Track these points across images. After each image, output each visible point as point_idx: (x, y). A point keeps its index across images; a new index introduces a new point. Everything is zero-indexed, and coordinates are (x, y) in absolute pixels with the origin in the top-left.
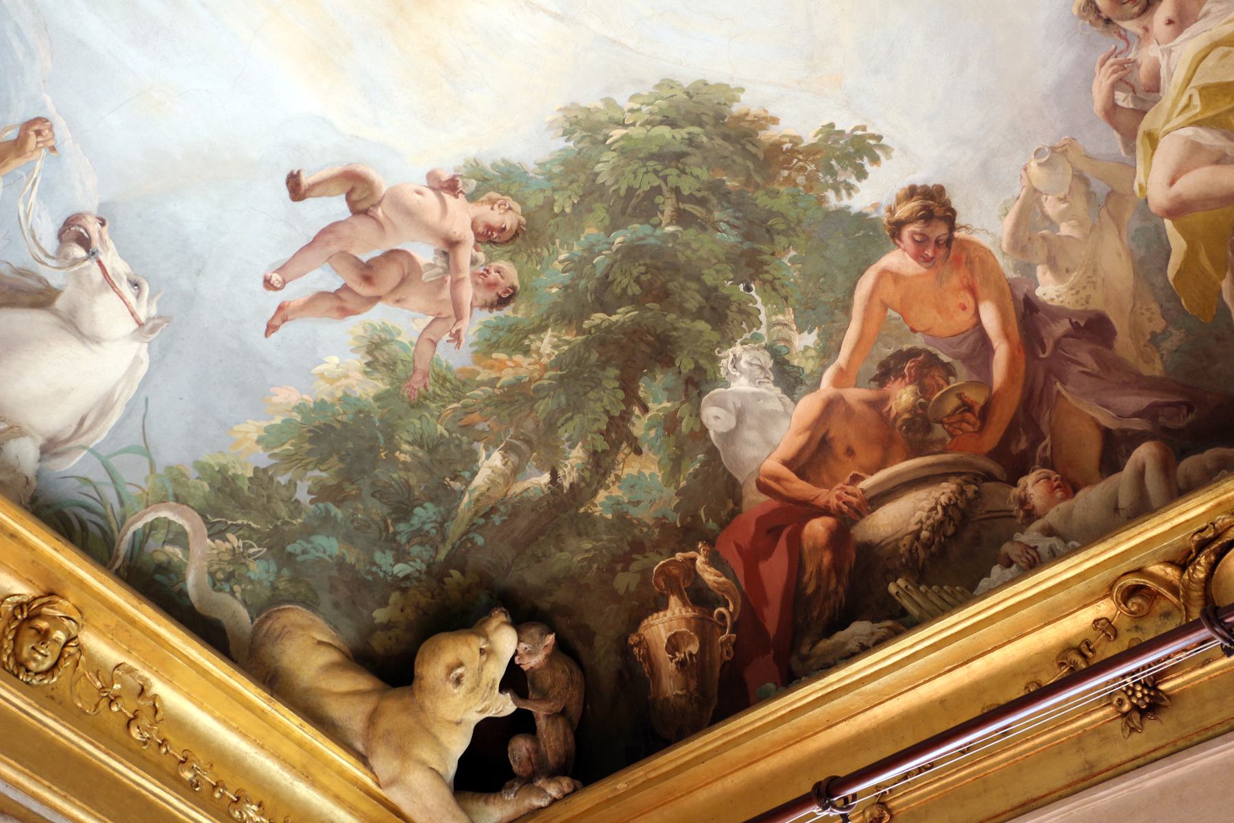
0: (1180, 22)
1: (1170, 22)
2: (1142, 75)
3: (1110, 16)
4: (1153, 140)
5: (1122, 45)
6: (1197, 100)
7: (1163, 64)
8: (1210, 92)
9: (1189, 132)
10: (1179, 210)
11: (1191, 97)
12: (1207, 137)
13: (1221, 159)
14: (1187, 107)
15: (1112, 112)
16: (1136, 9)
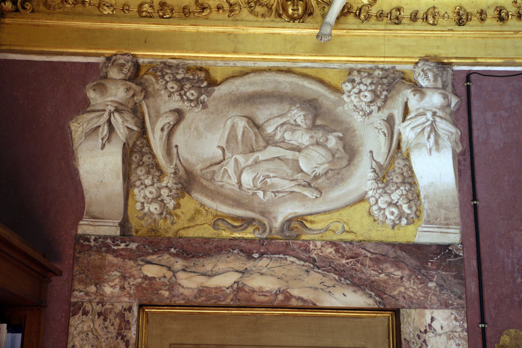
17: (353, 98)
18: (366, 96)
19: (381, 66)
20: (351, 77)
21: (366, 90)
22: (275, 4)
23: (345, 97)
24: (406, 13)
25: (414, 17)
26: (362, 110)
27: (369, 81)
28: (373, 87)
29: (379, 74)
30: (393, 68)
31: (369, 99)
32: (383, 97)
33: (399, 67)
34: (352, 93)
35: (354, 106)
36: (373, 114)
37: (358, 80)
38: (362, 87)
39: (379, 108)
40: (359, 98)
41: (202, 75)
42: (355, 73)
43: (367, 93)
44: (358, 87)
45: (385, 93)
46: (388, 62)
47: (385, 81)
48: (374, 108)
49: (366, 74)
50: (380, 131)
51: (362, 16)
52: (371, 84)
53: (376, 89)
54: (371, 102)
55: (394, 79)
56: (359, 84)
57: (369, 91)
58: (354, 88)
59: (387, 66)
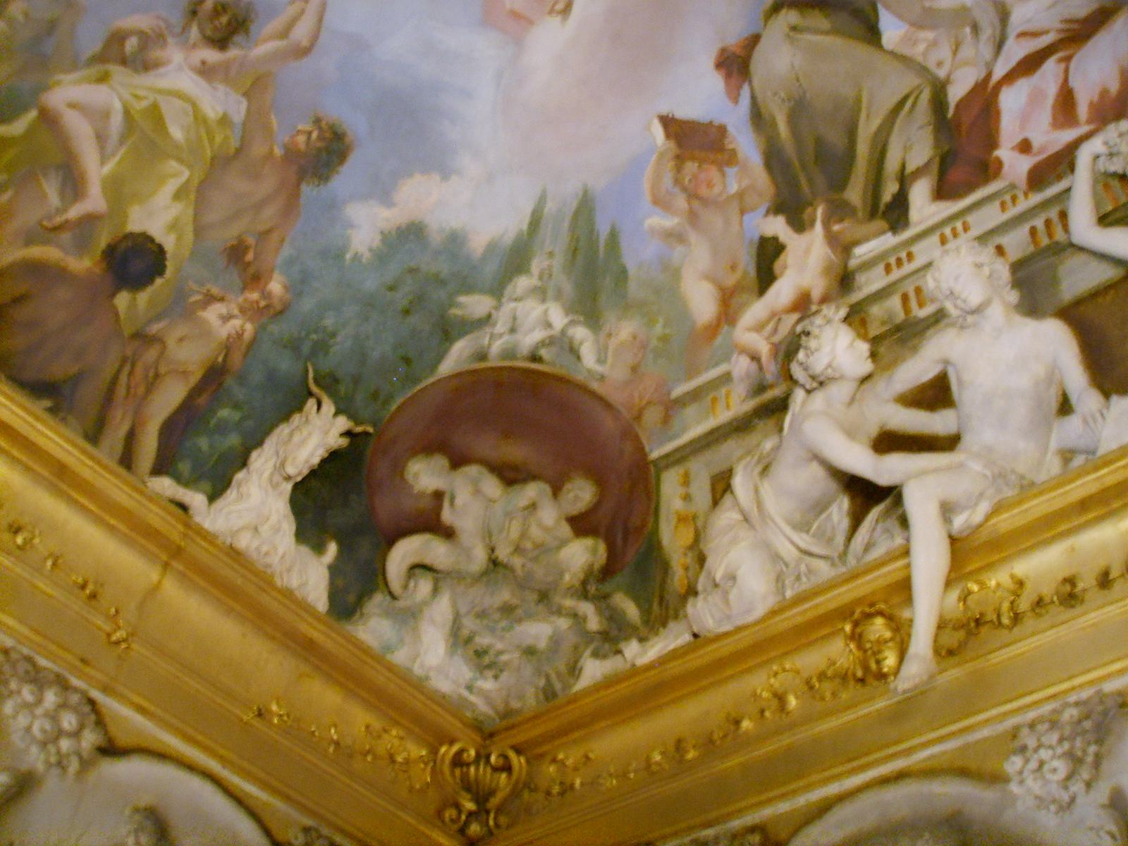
0: (205, 71)
1: (203, 63)
2: (156, 54)
3: (200, 14)
4: (103, 79)
5: (178, 30)
6: (144, 104)
7: (171, 67)
8: (155, 114)
9: (118, 105)
10: (48, 119)
11: (145, 98)
12: (117, 120)
13: (101, 138)
14: (136, 96)
15: (118, 38)
16: (209, 33)
17: (1030, 782)
18: (1055, 770)
19: (1073, 698)
20: (1017, 743)
21: (1053, 757)
22: (852, 667)
23: (1014, 788)
24: (1087, 582)
25: (1105, 581)
26: (1054, 801)
27: (1053, 738)
28: (1066, 746)
29: (1072, 716)
30: (1099, 692)
31: (1062, 772)
32: (1090, 759)
33: (1109, 687)
34: (1026, 774)
35: (1037, 797)
36: (1079, 800)
37: (1031, 743)
38: (1044, 754)
39: (1088, 785)
40: (1043, 778)
41: (756, 839)
42: (1025, 731)
43: (1056, 763)
44: (1036, 756)
45: (1092, 749)
46: (1081, 686)
47: (1087, 724)
48: (1077, 787)
49: (1046, 726)
50: (1102, 834)
51: (1005, 621)
52: (1061, 740)
53: (1072, 747)
54: (1069, 777)
55: (1105, 713)
56: (1036, 750)
57: (1059, 757)
58: (1027, 761)
59: (1085, 694)
